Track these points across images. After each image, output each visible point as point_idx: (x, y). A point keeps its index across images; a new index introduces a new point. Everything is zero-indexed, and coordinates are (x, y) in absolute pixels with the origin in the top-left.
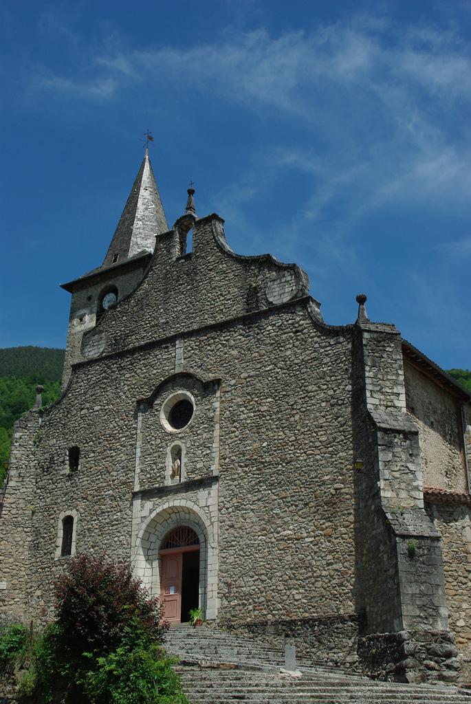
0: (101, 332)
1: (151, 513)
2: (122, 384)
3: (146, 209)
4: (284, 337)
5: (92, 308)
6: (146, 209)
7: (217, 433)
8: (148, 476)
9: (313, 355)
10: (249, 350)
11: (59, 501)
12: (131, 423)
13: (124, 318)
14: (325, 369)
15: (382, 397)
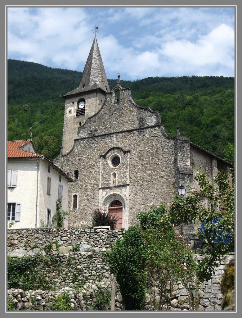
0: (85, 128)
1: (106, 195)
2: (94, 149)
3: (96, 63)
4: (152, 138)
5: (74, 108)
6: (96, 63)
7: (128, 170)
8: (104, 183)
9: (161, 145)
10: (140, 141)
11: (71, 189)
12: (97, 163)
13: (94, 123)
14: (165, 151)
15: (183, 162)
